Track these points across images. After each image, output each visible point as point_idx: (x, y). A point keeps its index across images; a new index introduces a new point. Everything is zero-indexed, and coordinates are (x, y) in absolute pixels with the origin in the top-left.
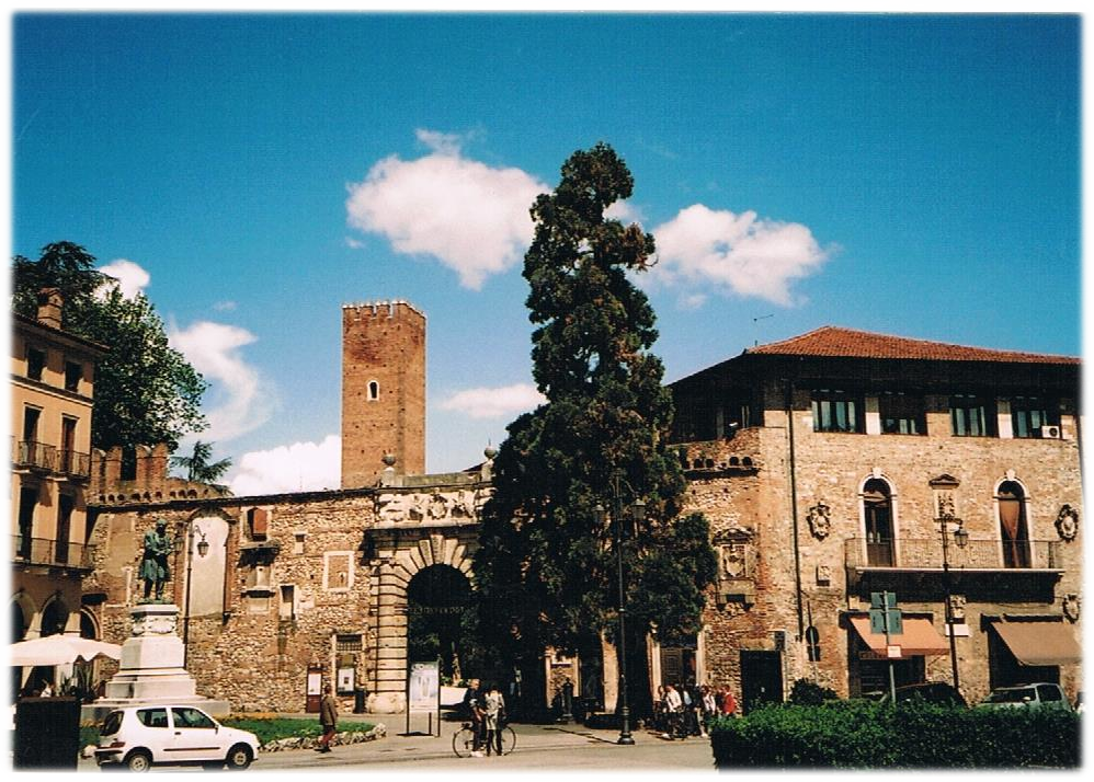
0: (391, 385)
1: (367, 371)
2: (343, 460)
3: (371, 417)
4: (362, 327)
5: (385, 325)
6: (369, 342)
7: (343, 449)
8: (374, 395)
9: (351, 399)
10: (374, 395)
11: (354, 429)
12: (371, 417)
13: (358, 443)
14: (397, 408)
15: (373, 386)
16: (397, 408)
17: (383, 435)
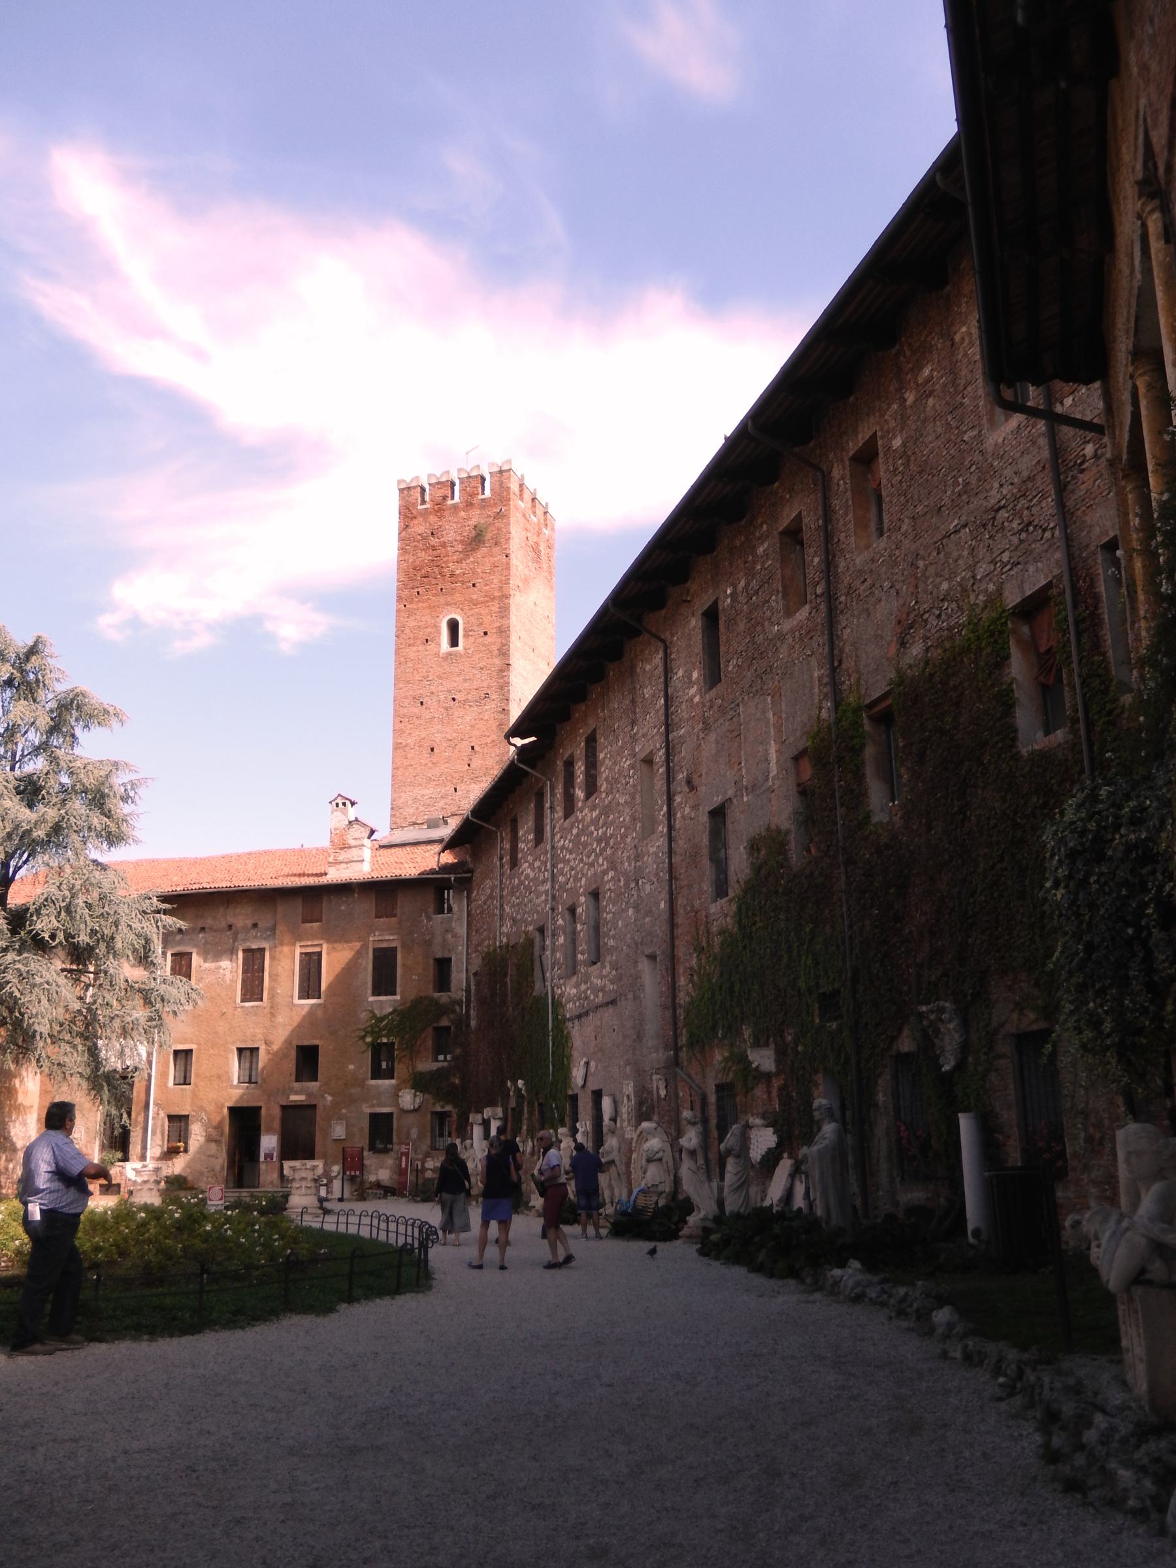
0: (487, 619)
1: (442, 599)
2: (395, 769)
3: (448, 685)
4: (433, 519)
5: (476, 512)
6: (444, 545)
7: (397, 747)
8: (454, 642)
9: (412, 652)
10: (454, 642)
11: (417, 710)
12: (448, 685)
13: (423, 734)
14: (497, 661)
15: (453, 626)
16: (497, 661)
17: (470, 714)
